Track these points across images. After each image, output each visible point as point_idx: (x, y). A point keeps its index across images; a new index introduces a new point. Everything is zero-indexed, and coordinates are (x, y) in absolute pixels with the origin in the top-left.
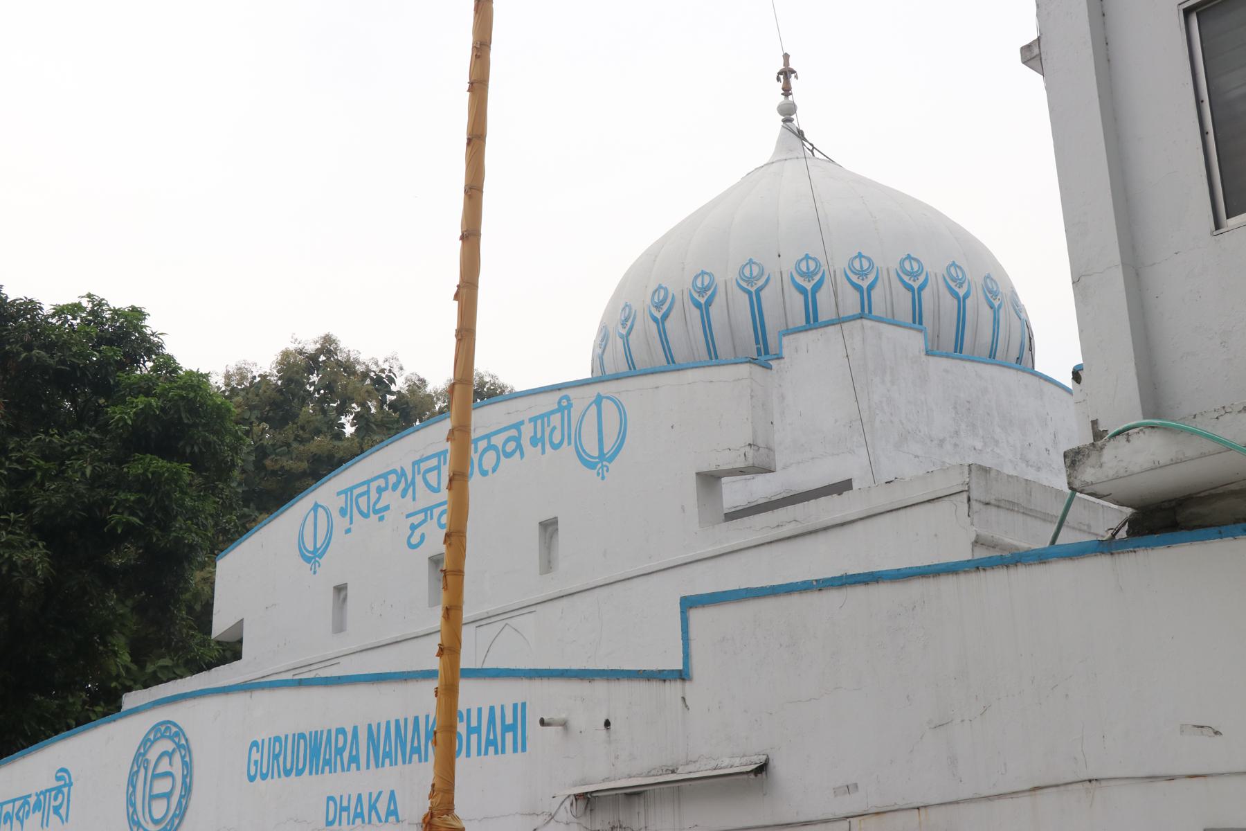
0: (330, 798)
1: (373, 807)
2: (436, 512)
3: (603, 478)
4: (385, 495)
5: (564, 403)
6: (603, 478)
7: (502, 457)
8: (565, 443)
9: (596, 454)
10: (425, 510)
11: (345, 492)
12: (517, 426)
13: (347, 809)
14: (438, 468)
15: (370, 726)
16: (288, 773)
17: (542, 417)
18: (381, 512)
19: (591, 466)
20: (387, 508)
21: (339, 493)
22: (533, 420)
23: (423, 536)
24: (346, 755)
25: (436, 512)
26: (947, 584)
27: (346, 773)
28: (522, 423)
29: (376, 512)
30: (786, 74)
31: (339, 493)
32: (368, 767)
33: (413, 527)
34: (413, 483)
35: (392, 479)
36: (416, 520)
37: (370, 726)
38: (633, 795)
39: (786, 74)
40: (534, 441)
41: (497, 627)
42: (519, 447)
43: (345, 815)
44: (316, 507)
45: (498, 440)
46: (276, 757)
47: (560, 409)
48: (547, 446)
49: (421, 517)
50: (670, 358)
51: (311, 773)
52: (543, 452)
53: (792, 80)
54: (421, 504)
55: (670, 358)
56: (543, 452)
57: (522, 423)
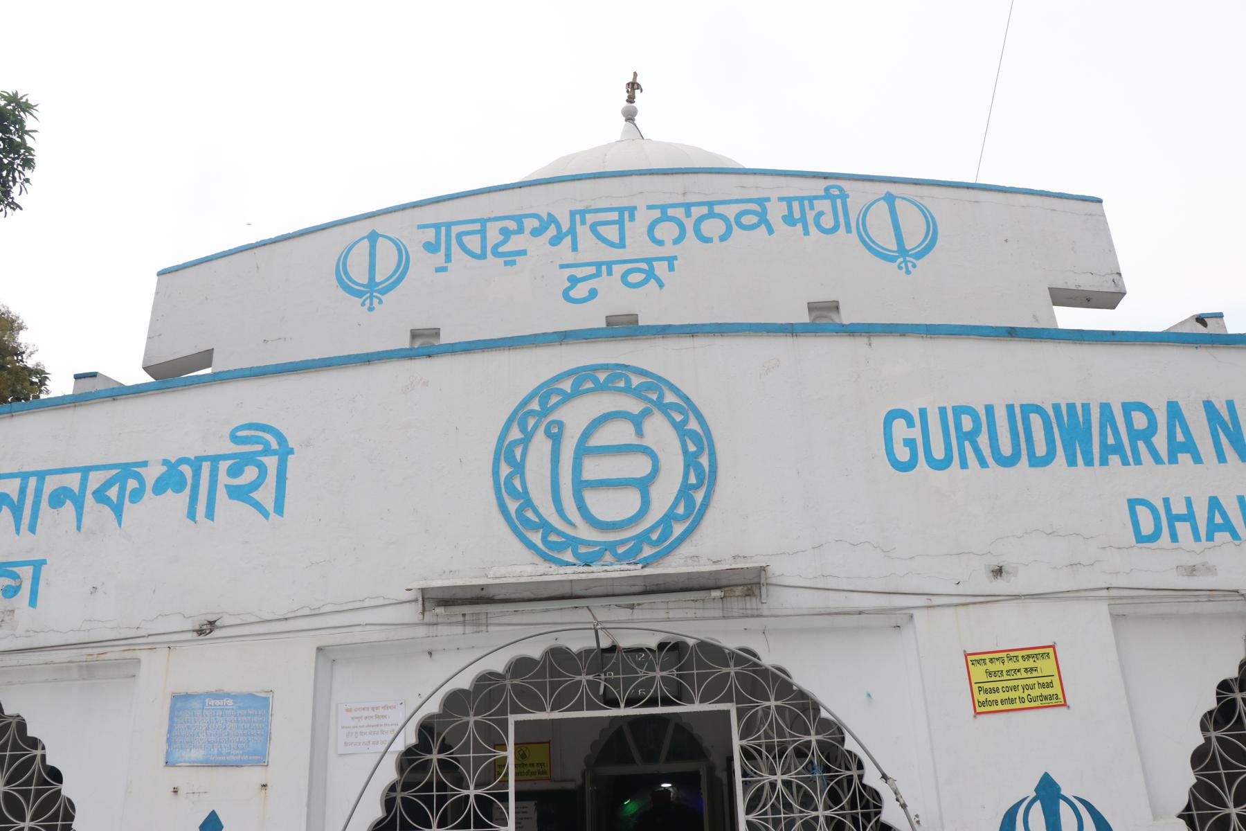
0: (1133, 503)
2: (618, 270)
3: (908, 272)
4: (514, 238)
5: (836, 192)
6: (908, 272)
7: (735, 228)
8: (842, 229)
9: (895, 248)
10: (598, 265)
11: (437, 227)
12: (761, 202)
13: (1190, 517)
14: (620, 223)
15: (1209, 406)
16: (1009, 462)
17: (801, 200)
18: (511, 259)
19: (892, 259)
20: (523, 253)
21: (420, 227)
22: (789, 201)
23: (593, 294)
24: (1160, 441)
25: (618, 270)
27: (1166, 469)
28: (768, 199)
29: (496, 254)
30: (633, 86)
31: (420, 227)
32: (1221, 458)
33: (574, 281)
34: (572, 231)
36: (579, 272)
37: (1209, 406)
39: (633, 86)
40: (789, 220)
42: (763, 220)
43: (1183, 528)
44: (373, 237)
45: (731, 211)
46: (972, 436)
47: (827, 195)
48: (813, 229)
49: (592, 270)
51: (1072, 462)
52: (806, 232)
53: (637, 92)
54: (583, 257)
56: (806, 232)
57: (768, 199)
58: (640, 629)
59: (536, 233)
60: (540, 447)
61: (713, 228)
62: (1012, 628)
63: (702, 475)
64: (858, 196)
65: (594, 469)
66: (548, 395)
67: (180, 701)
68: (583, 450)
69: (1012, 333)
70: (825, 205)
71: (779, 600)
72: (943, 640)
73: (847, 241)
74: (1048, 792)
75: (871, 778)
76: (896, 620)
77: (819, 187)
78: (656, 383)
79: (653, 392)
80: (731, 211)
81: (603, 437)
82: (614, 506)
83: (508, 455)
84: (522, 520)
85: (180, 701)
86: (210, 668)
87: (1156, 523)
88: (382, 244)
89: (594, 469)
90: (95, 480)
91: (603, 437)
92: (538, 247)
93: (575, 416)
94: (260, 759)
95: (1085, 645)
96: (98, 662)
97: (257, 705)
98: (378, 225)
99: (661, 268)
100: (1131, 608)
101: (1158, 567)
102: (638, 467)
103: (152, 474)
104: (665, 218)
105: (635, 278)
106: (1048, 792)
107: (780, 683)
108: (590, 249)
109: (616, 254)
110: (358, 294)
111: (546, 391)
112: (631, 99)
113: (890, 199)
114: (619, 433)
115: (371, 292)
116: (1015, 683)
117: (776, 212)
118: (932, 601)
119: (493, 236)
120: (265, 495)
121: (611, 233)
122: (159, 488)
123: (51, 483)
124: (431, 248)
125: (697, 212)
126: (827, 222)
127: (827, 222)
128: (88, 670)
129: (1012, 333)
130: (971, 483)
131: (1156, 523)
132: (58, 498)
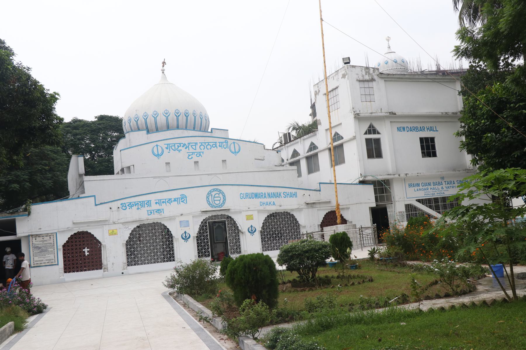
1: (270, 203)
2: (195, 154)
12: (216, 143)
18: (180, 151)
22: (219, 143)
25: (195, 154)
26: (349, 185)
30: (164, 63)
33: (189, 155)
35: (182, 145)
36: (190, 154)
38: (314, 203)
39: (164, 63)
40: (220, 146)
41: (213, 176)
42: (216, 145)
44: (157, 146)
50: (200, 129)
55: (200, 129)
58: (219, 213)
59: (183, 147)
60: (210, 197)
61: (209, 147)
62: (250, 213)
63: (225, 199)
64: (230, 142)
65: (215, 199)
66: (210, 192)
67: (180, 222)
68: (214, 197)
69: (252, 186)
70: (225, 144)
71: (231, 211)
72: (244, 214)
73: (228, 150)
74: (252, 226)
75: (238, 225)
76: (240, 212)
77: (223, 140)
78: (220, 190)
79: (220, 191)
80: (211, 144)
81: (216, 196)
82: (217, 202)
83: (207, 198)
84: (209, 204)
85: (180, 222)
86: (183, 218)
87: (262, 204)
88: (159, 147)
89: (215, 199)
90: (167, 200)
91: (216, 196)
92: (183, 149)
93: (213, 193)
94: (189, 226)
95: (255, 214)
96: (171, 218)
97: (188, 221)
98: (158, 143)
99: (201, 153)
100: (259, 211)
101: (262, 208)
102: (219, 199)
103: (173, 200)
104: (202, 145)
105: (198, 155)
106: (252, 226)
107: (230, 217)
108: (191, 150)
109: (195, 151)
110: (156, 156)
111: (210, 191)
112: (163, 66)
113: (234, 143)
114: (217, 195)
115: (158, 156)
116: (249, 218)
117: (218, 144)
118: (243, 211)
119: (176, 147)
120: (185, 201)
121: (194, 147)
122: (174, 201)
123: (162, 201)
124: (167, 148)
125: (207, 144)
126: (225, 147)
127: (225, 147)
128: (170, 219)
129: (252, 186)
130: (247, 200)
131: (262, 204)
132: (163, 202)
